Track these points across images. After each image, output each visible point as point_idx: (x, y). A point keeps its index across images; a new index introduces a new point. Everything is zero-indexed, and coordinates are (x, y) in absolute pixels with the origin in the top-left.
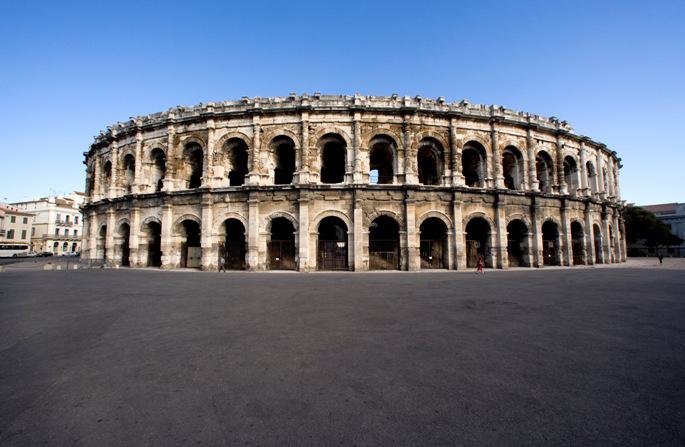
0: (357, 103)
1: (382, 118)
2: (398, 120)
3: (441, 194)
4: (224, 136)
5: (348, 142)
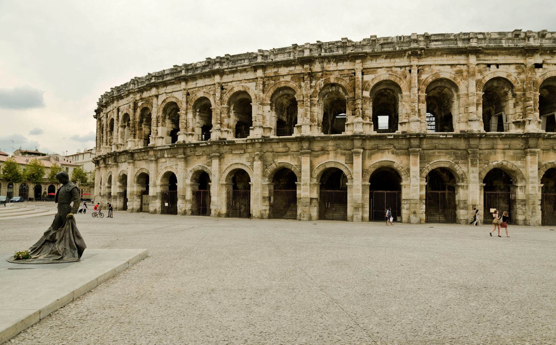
1: (283, 71)
2: (298, 69)
3: (341, 142)
5: (253, 97)
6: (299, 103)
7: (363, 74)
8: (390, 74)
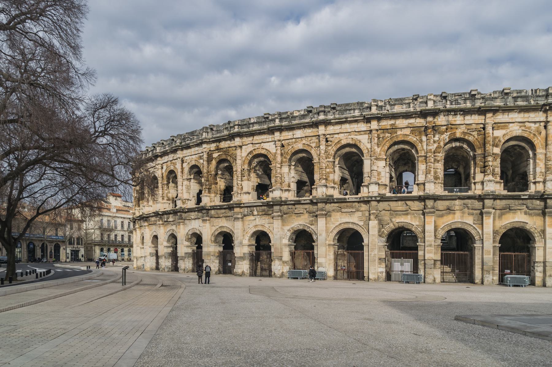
0: (374, 110)
1: (401, 123)
4: (251, 152)
5: (365, 152)
6: (420, 159)
7: (493, 128)
8: (523, 130)
